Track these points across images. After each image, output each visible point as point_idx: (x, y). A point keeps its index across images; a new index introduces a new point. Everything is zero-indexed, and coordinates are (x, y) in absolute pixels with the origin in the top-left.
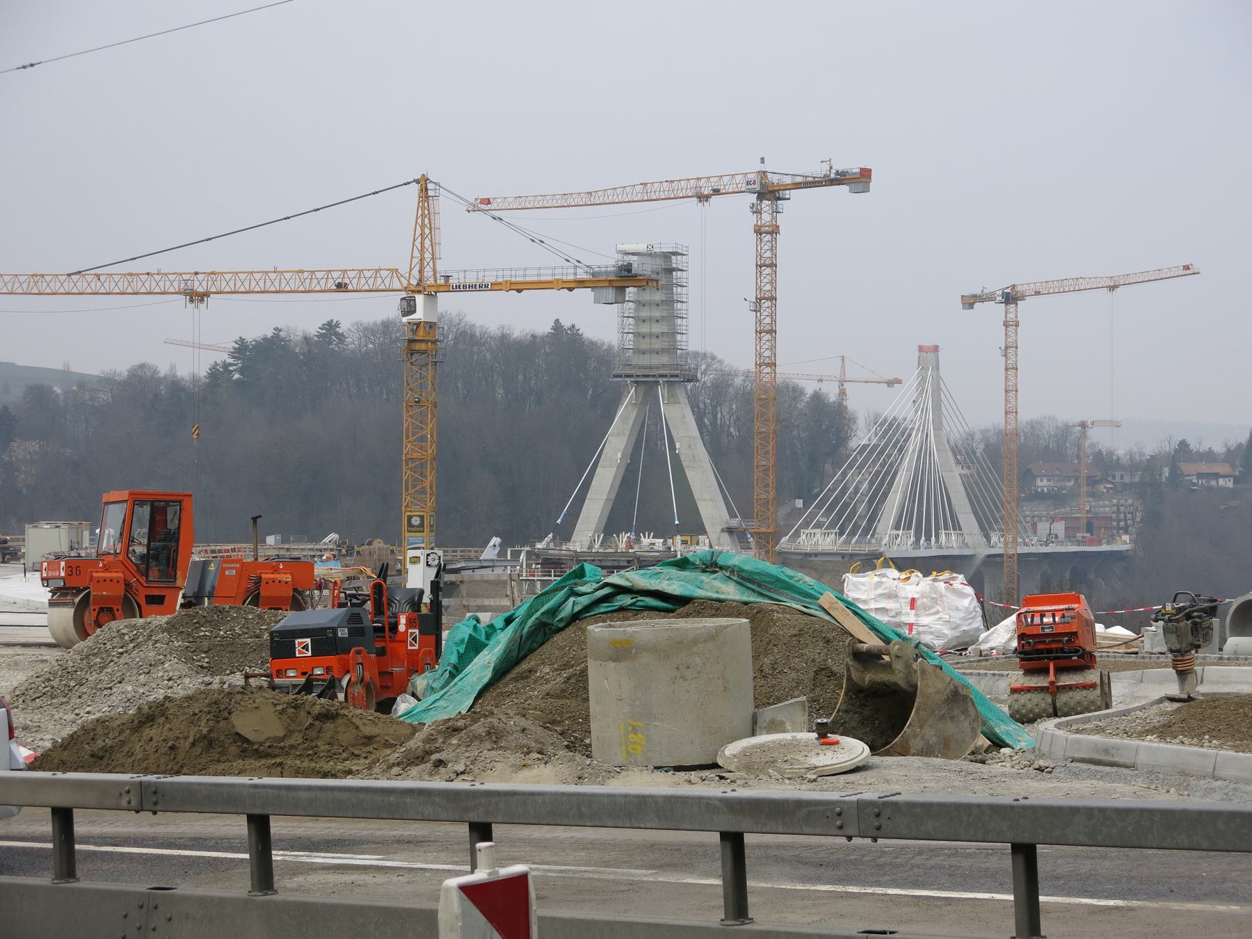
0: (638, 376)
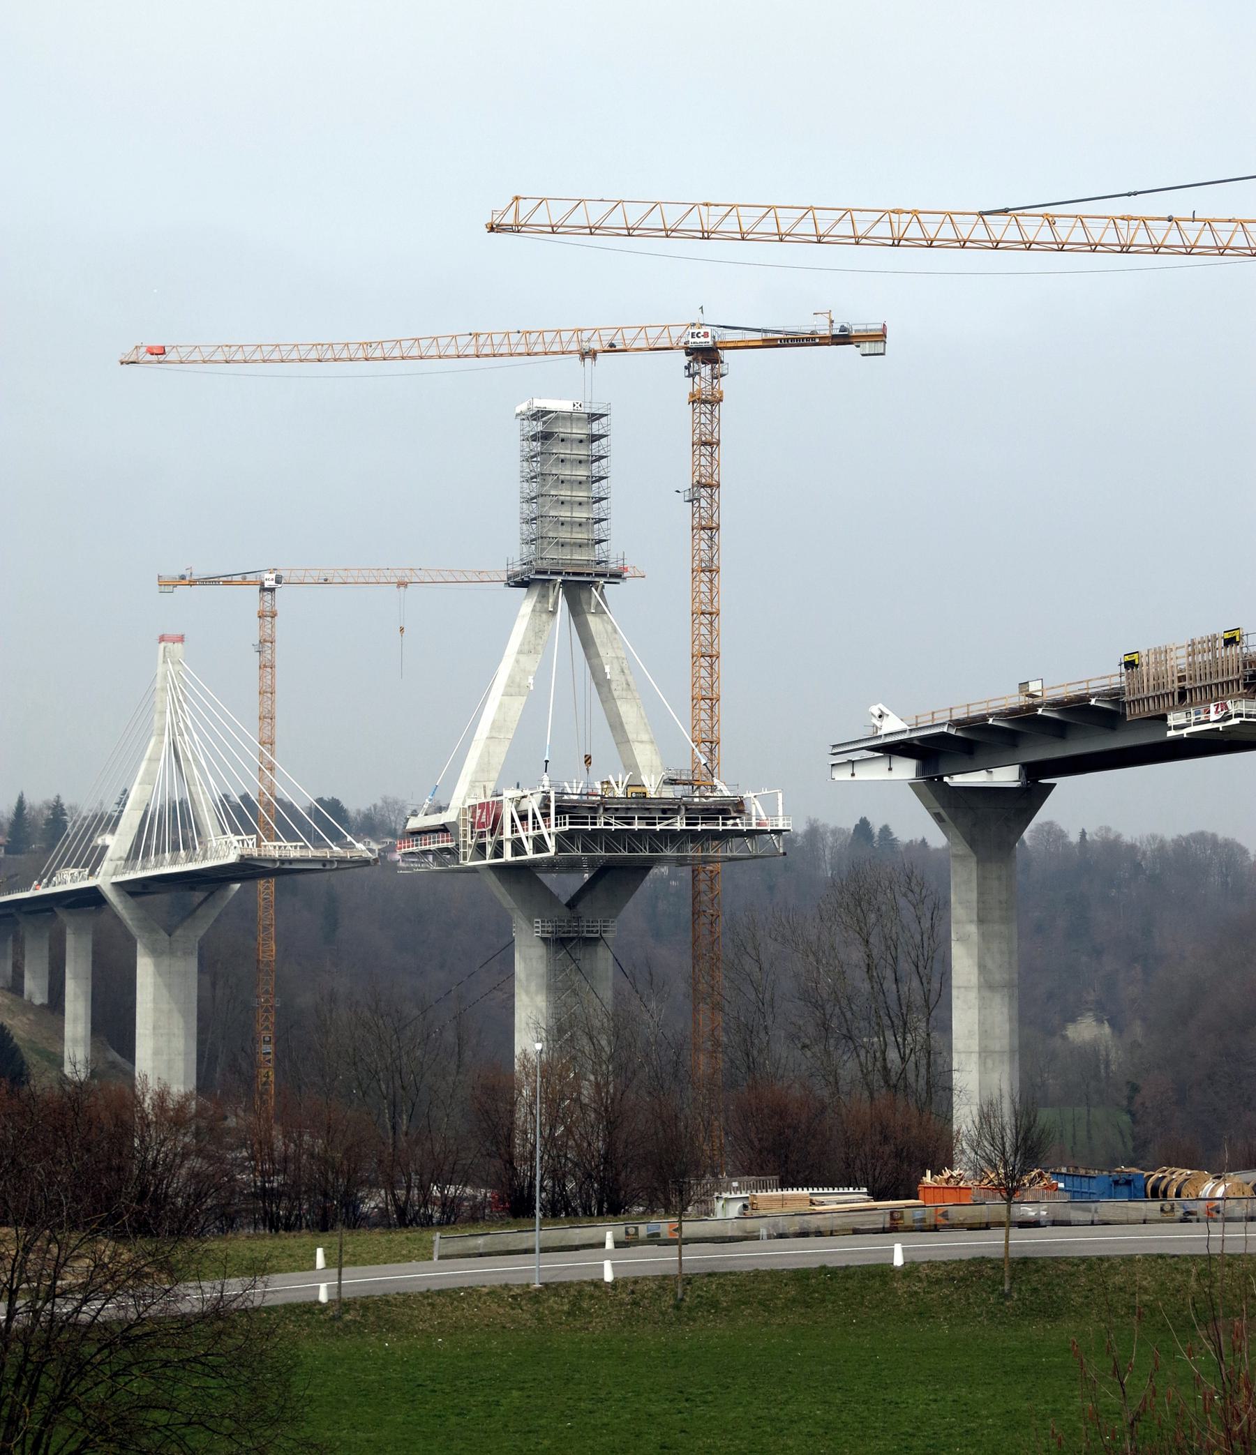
0: (568, 573)
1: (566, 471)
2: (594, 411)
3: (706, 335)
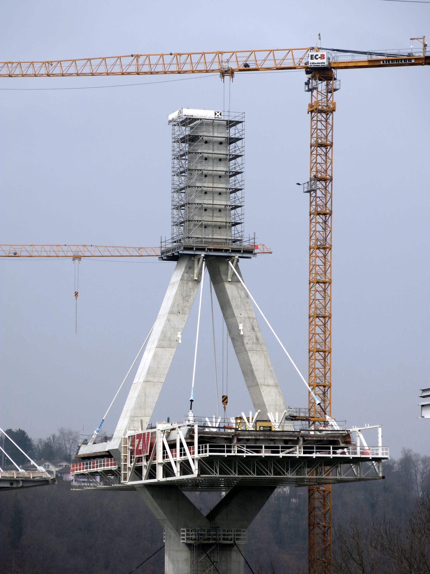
0: (210, 250)
1: (208, 167)
2: (231, 119)
3: (322, 57)
